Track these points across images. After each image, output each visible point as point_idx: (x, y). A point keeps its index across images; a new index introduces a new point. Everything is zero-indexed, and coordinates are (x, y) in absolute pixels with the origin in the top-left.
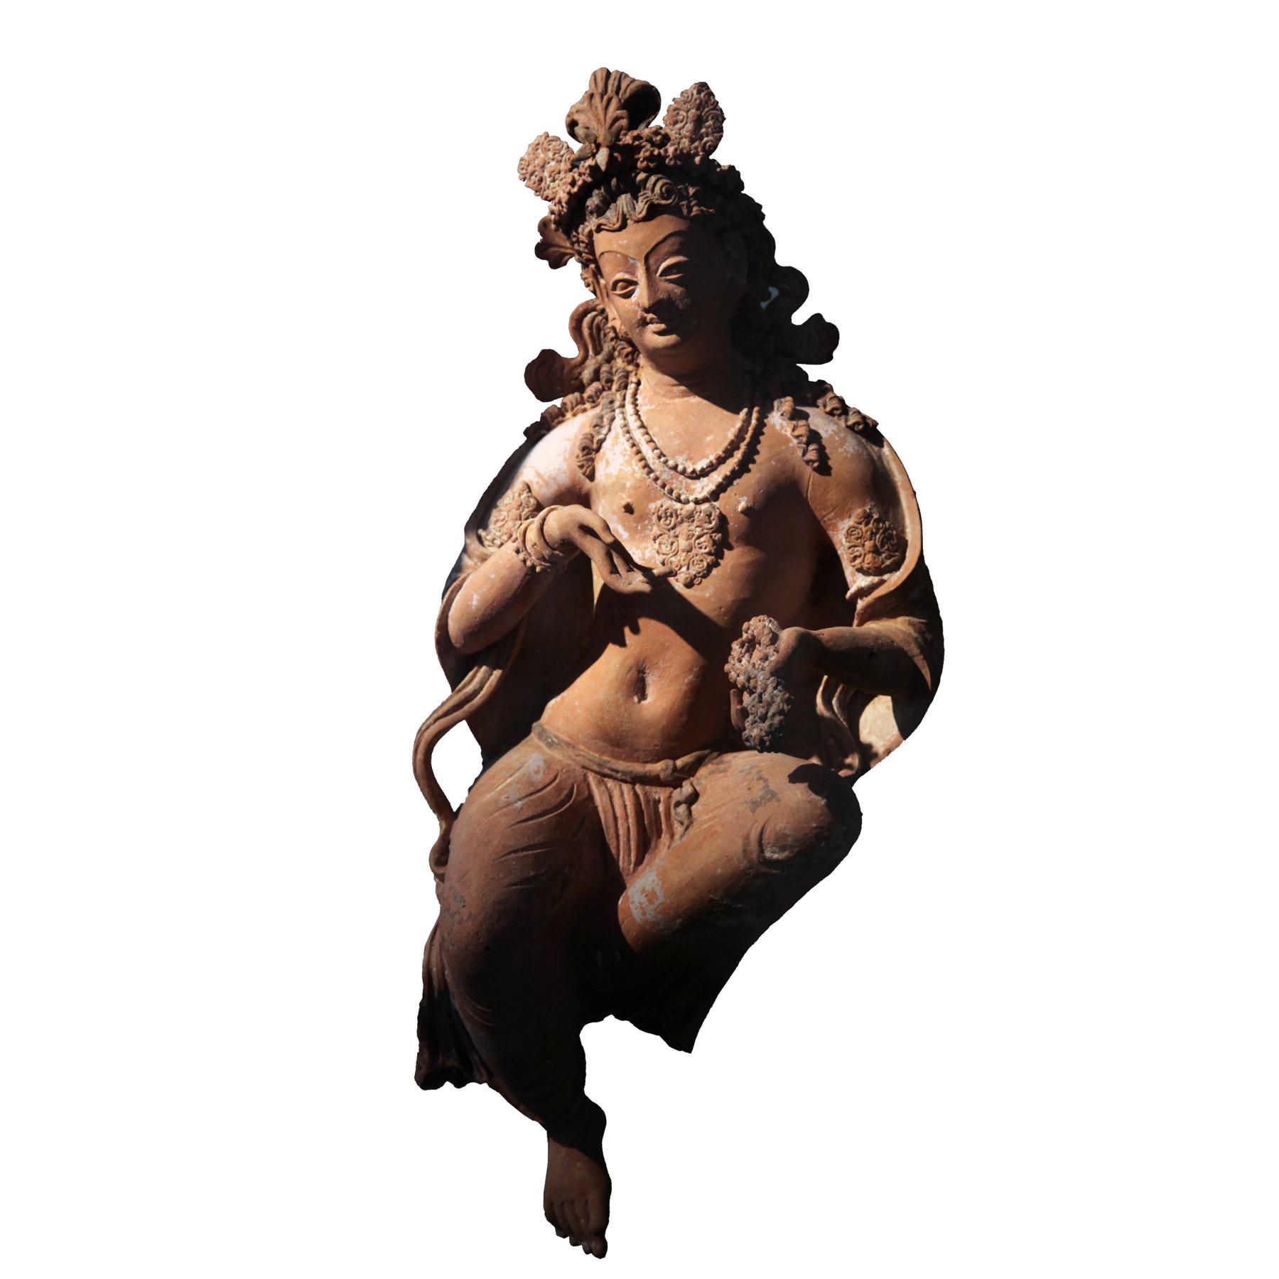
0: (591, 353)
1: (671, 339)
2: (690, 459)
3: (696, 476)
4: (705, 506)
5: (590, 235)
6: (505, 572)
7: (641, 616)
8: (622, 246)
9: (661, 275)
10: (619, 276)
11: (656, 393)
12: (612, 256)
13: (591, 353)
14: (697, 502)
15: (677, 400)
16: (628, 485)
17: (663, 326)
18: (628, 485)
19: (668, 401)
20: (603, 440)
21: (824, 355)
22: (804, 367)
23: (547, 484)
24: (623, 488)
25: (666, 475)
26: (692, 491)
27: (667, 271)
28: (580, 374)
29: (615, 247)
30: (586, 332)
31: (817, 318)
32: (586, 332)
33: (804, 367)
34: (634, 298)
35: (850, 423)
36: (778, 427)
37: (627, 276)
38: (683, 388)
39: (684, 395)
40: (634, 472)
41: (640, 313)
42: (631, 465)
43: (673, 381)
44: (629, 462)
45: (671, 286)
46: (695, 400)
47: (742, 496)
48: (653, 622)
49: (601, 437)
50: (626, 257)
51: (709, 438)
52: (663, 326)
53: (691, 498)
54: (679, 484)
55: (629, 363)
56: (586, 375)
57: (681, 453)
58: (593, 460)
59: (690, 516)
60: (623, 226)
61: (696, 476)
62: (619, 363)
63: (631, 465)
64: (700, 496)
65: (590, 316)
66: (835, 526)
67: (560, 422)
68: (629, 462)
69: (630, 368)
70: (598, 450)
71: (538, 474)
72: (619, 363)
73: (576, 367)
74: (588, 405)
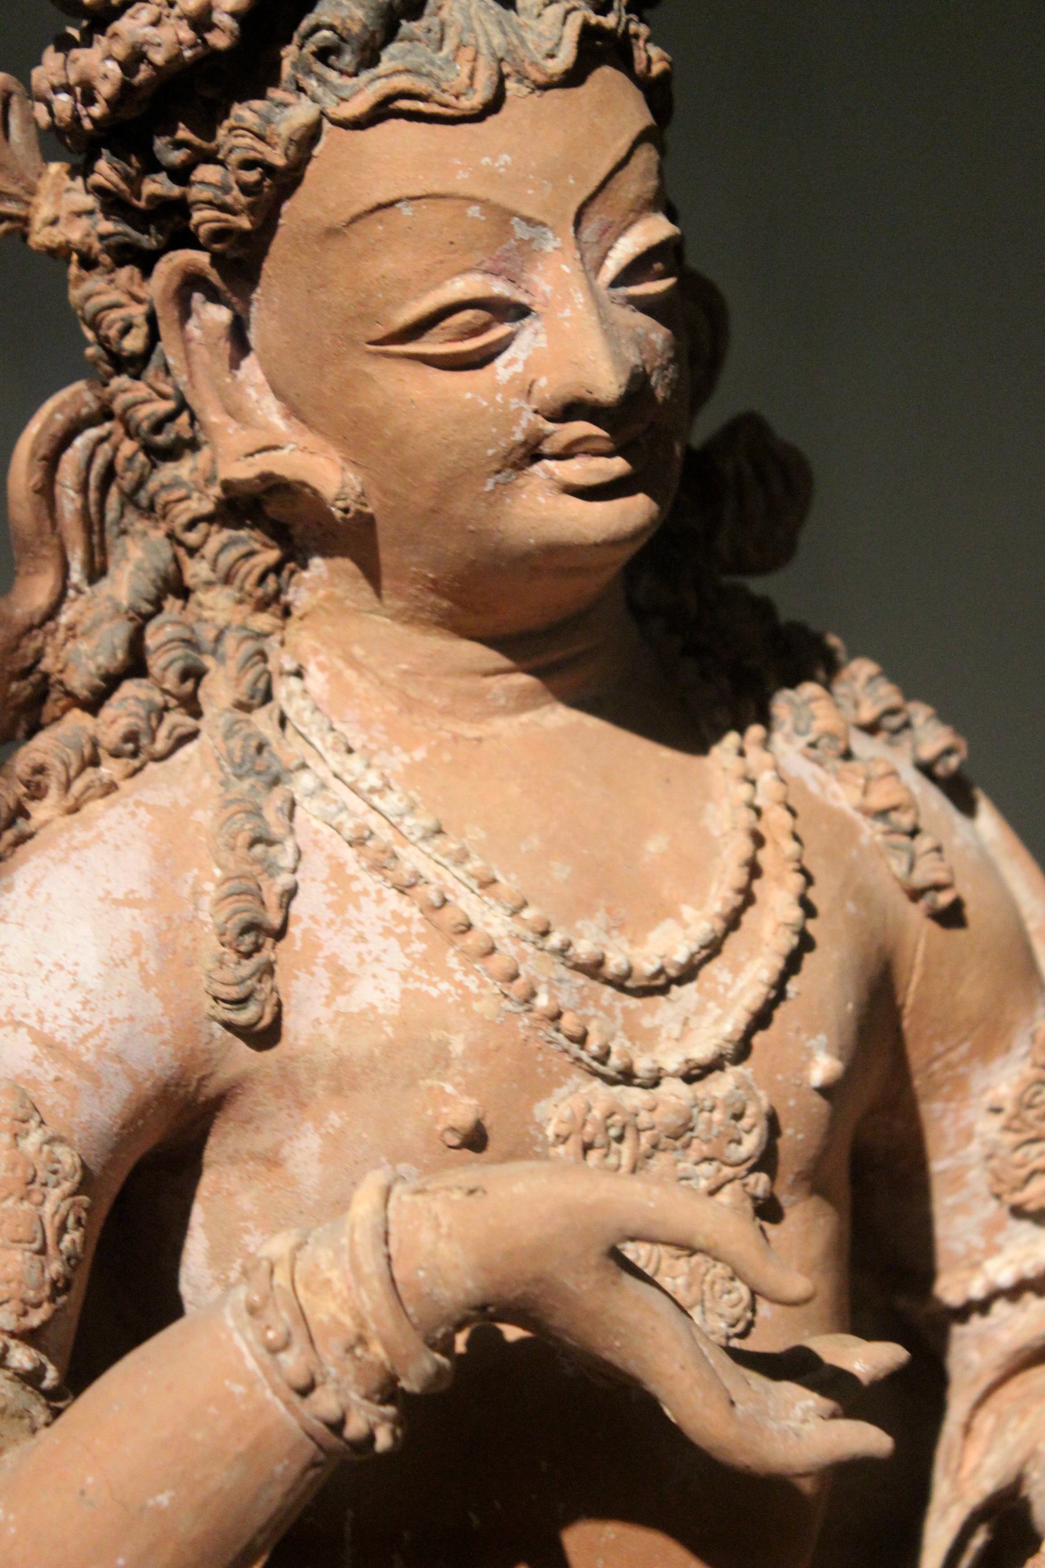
0: (76, 575)
1: (635, 510)
2: (616, 926)
3: (658, 986)
4: (722, 1085)
5: (311, 135)
6: (222, 1477)
7: (570, 1518)
8: (491, 177)
9: (615, 283)
10: (460, 288)
11: (409, 705)
12: (442, 213)
13: (76, 575)
14: (695, 1074)
15: (501, 725)
16: (458, 1046)
17: (618, 466)
18: (458, 1046)
19: (470, 731)
20: (292, 893)
21: (778, 553)
22: (757, 586)
23: (95, 1079)
24: (441, 1058)
25: (569, 991)
26: (648, 1038)
27: (636, 270)
28: (39, 655)
29: (461, 181)
30: (69, 501)
31: (748, 429)
32: (69, 501)
33: (757, 586)
34: (501, 369)
35: (928, 750)
36: (813, 787)
37: (499, 288)
38: (523, 679)
39: (523, 703)
40: (467, 996)
41: (527, 421)
42: (448, 974)
43: (494, 659)
44: (430, 963)
45: (642, 321)
46: (559, 717)
47: (813, 1032)
48: (611, 1531)
49: (284, 880)
50: (502, 216)
51: (655, 845)
52: (618, 466)
53: (672, 1062)
54: (606, 1017)
55: (263, 605)
56: (83, 653)
57: (587, 909)
58: (269, 969)
59: (682, 1132)
60: (494, 105)
61: (658, 986)
62: (217, 606)
63: (448, 974)
64: (702, 1051)
65: (79, 442)
66: (960, 1085)
67: (23, 839)
68: (430, 963)
69: (264, 621)
70: (280, 934)
71: (50, 1046)
72: (217, 606)
73: (29, 629)
74: (110, 769)
